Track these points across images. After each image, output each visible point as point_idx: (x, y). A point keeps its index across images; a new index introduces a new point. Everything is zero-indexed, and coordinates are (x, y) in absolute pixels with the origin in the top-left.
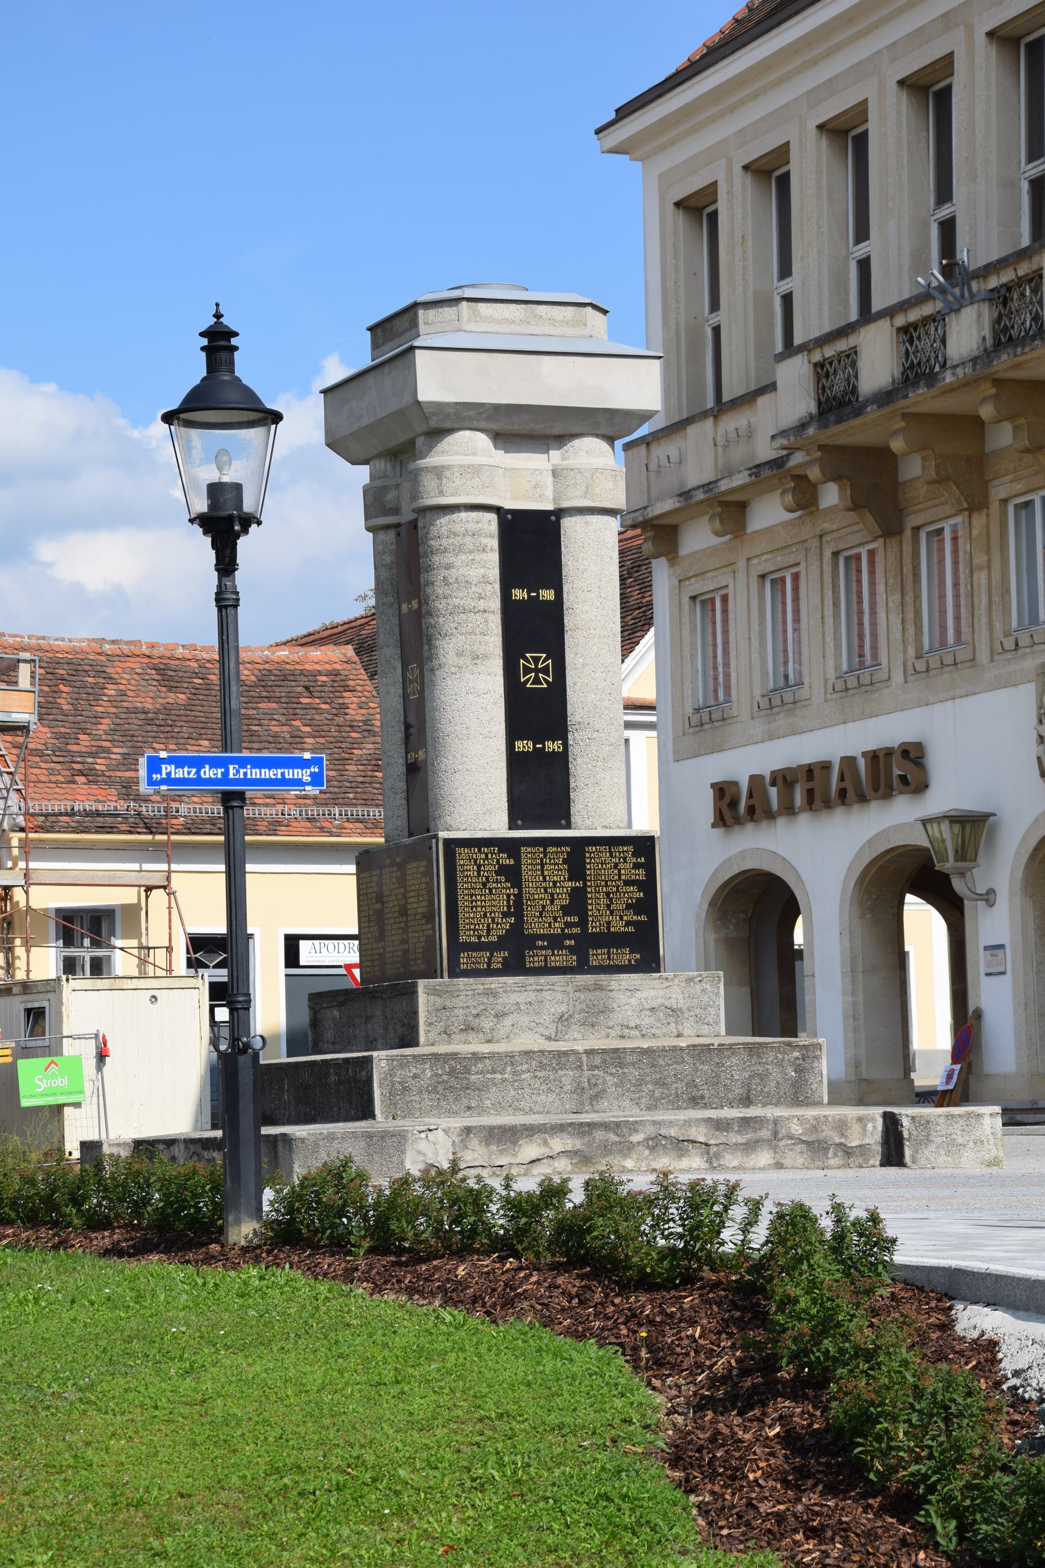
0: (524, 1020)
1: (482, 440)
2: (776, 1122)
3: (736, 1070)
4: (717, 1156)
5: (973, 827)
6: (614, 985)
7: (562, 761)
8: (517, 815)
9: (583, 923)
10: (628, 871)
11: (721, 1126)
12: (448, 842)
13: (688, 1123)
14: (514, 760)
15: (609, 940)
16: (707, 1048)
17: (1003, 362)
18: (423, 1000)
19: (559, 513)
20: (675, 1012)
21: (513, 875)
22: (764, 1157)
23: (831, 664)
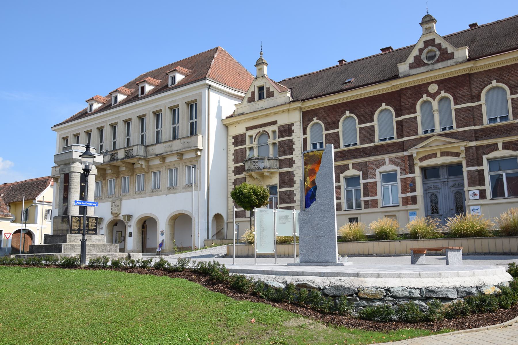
3: (108, 248)
10: (94, 221)
12: (72, 216)
15: (91, 230)
17: (112, 163)
18: (68, 237)
20: (100, 240)
21: (80, 221)
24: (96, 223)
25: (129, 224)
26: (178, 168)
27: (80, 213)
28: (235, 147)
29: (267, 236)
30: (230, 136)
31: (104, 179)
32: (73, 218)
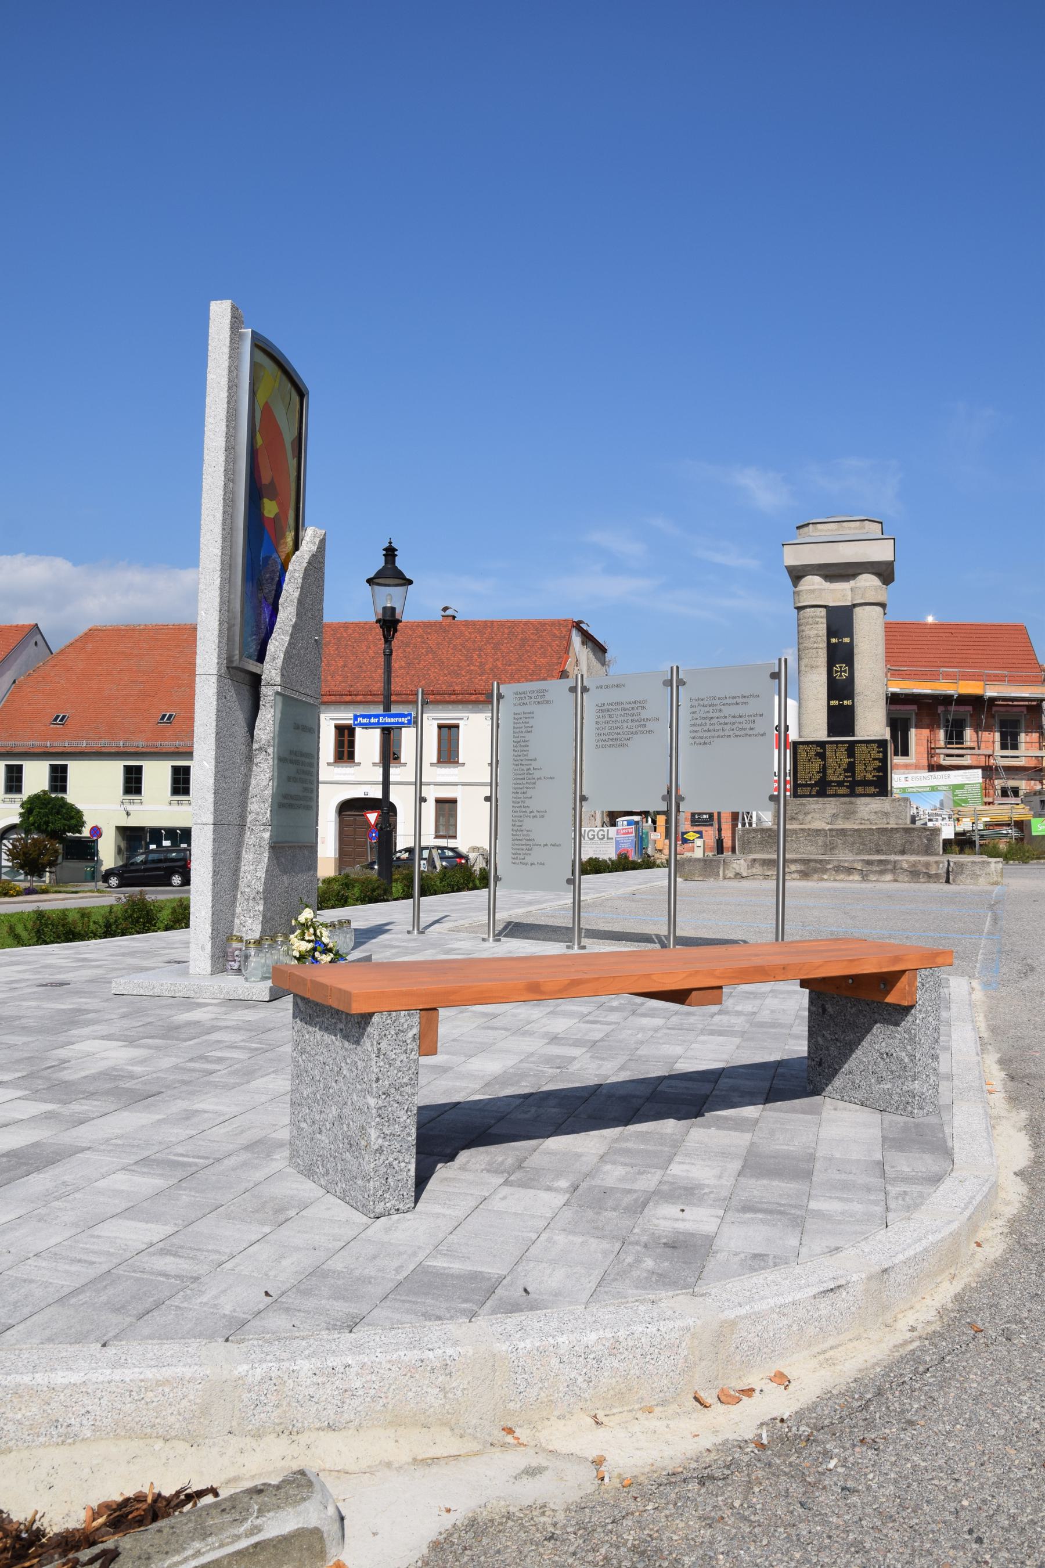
0: (817, 816)
1: (817, 579)
2: (895, 862)
4: (867, 875)
6: (858, 802)
7: (851, 709)
8: (831, 732)
9: (853, 775)
11: (869, 863)
13: (853, 861)
14: (831, 709)
15: (865, 783)
16: (886, 830)
19: (854, 606)
20: (886, 814)
21: (822, 756)
22: (889, 877)
24: (884, 761)
27: (832, 730)
29: (542, 814)
32: (800, 748)
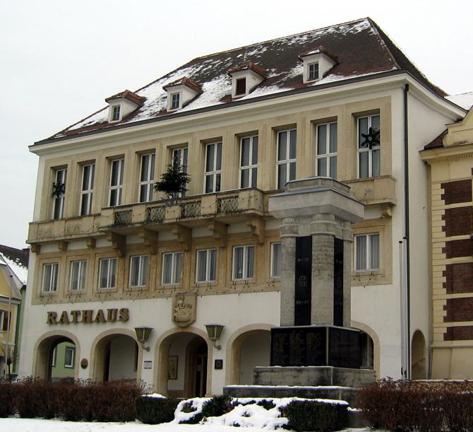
5: (145, 333)
23: (95, 285)
25: (146, 345)
26: (88, 261)
28: (446, 204)
30: (437, 182)
31: (155, 253)
